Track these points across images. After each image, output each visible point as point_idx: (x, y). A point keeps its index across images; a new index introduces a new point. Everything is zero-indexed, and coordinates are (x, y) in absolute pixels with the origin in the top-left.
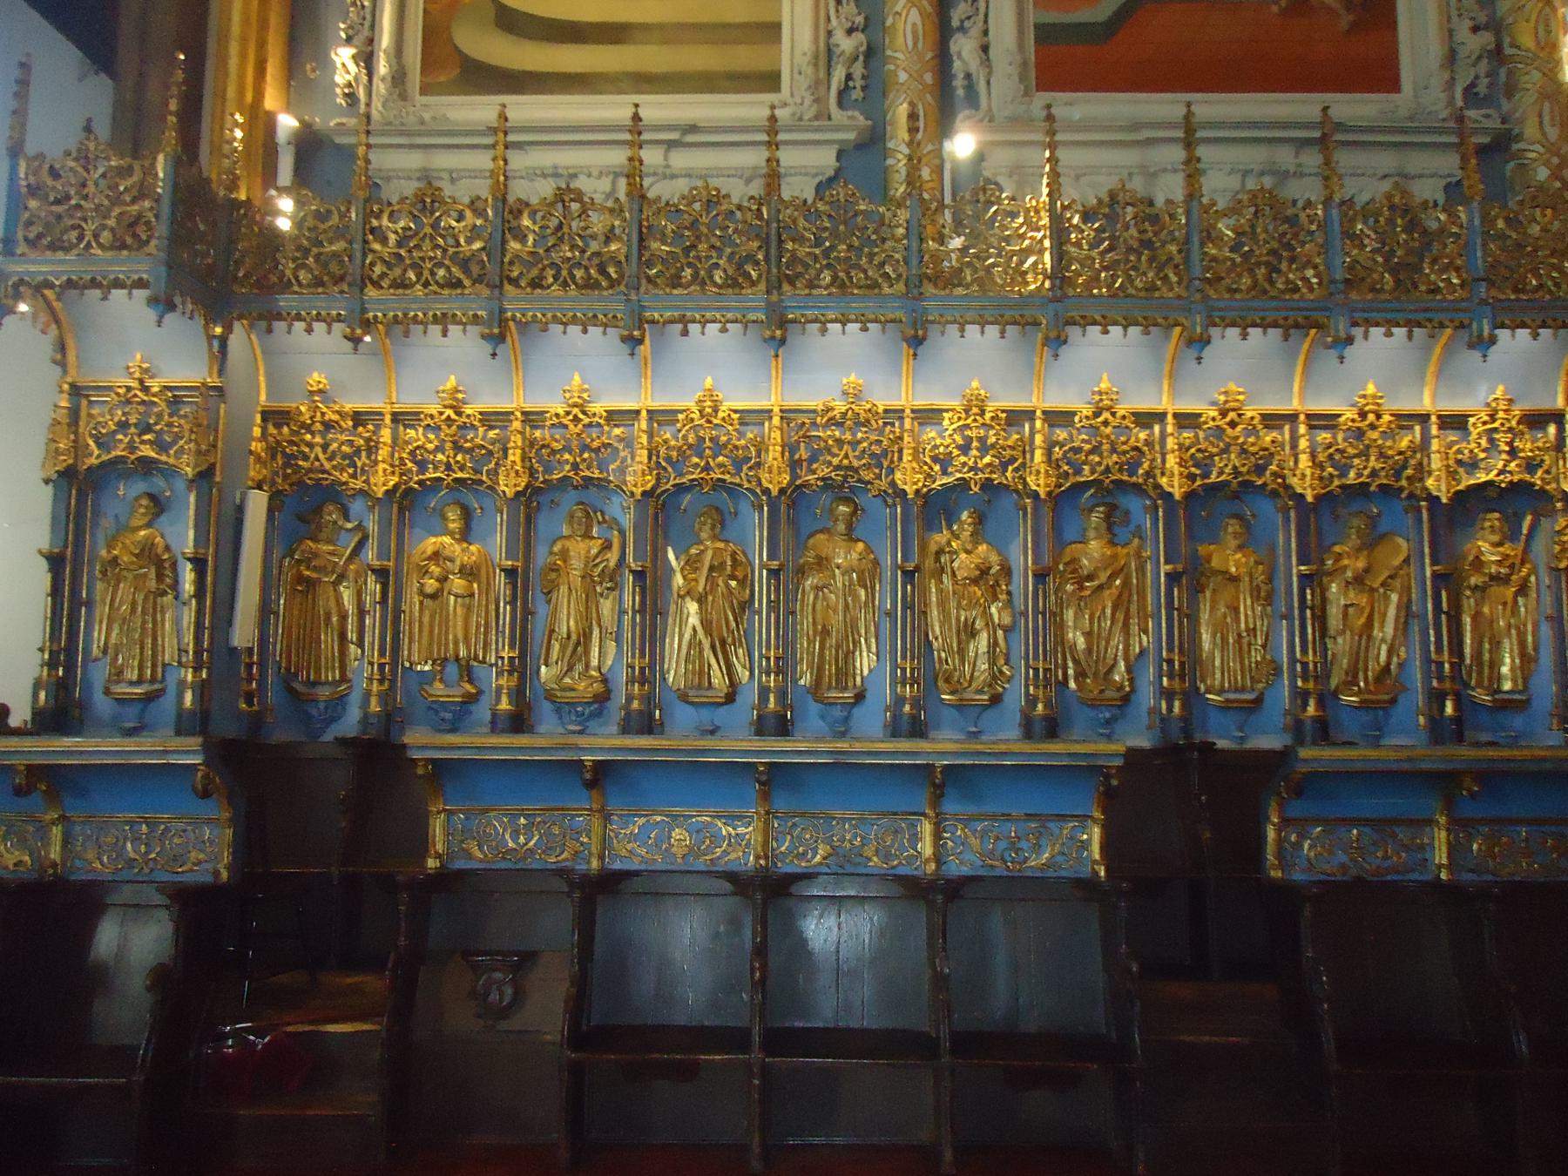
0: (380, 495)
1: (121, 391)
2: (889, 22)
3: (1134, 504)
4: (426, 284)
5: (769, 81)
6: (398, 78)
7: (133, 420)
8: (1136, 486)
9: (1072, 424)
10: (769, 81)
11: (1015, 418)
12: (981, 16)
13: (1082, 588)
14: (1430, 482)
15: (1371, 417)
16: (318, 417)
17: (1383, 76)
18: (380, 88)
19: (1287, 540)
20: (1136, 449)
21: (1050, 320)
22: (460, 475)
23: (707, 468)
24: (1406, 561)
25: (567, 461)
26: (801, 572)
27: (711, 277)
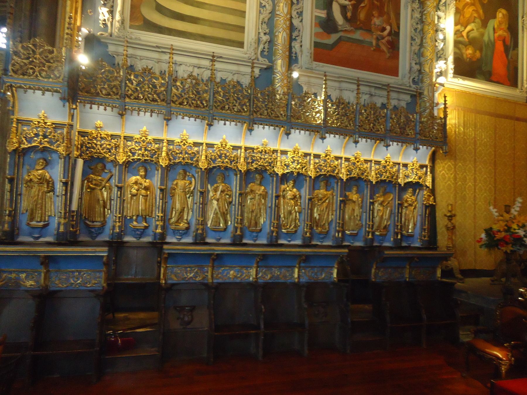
0: (121, 163)
1: (36, 123)
2: (277, 34)
3: (332, 181)
4: (146, 100)
5: (241, 45)
6: (123, 22)
7: (41, 134)
8: (334, 176)
9: (320, 158)
10: (241, 45)
11: (306, 155)
12: (300, 37)
13: (319, 202)
14: (399, 181)
15: (388, 163)
16: (99, 135)
17: (394, 72)
18: (117, 25)
19: (367, 192)
20: (335, 166)
21: (320, 131)
22: (146, 158)
23: (223, 162)
24: (392, 199)
25: (181, 157)
26: (246, 194)
27: (233, 109)
